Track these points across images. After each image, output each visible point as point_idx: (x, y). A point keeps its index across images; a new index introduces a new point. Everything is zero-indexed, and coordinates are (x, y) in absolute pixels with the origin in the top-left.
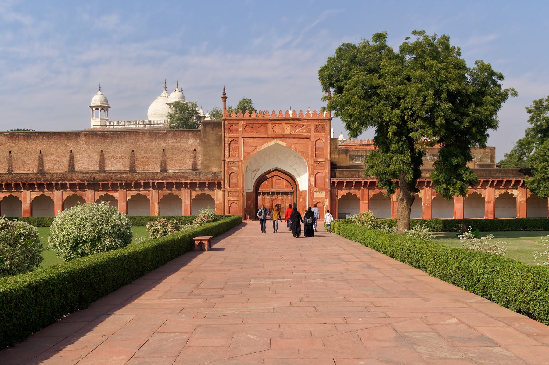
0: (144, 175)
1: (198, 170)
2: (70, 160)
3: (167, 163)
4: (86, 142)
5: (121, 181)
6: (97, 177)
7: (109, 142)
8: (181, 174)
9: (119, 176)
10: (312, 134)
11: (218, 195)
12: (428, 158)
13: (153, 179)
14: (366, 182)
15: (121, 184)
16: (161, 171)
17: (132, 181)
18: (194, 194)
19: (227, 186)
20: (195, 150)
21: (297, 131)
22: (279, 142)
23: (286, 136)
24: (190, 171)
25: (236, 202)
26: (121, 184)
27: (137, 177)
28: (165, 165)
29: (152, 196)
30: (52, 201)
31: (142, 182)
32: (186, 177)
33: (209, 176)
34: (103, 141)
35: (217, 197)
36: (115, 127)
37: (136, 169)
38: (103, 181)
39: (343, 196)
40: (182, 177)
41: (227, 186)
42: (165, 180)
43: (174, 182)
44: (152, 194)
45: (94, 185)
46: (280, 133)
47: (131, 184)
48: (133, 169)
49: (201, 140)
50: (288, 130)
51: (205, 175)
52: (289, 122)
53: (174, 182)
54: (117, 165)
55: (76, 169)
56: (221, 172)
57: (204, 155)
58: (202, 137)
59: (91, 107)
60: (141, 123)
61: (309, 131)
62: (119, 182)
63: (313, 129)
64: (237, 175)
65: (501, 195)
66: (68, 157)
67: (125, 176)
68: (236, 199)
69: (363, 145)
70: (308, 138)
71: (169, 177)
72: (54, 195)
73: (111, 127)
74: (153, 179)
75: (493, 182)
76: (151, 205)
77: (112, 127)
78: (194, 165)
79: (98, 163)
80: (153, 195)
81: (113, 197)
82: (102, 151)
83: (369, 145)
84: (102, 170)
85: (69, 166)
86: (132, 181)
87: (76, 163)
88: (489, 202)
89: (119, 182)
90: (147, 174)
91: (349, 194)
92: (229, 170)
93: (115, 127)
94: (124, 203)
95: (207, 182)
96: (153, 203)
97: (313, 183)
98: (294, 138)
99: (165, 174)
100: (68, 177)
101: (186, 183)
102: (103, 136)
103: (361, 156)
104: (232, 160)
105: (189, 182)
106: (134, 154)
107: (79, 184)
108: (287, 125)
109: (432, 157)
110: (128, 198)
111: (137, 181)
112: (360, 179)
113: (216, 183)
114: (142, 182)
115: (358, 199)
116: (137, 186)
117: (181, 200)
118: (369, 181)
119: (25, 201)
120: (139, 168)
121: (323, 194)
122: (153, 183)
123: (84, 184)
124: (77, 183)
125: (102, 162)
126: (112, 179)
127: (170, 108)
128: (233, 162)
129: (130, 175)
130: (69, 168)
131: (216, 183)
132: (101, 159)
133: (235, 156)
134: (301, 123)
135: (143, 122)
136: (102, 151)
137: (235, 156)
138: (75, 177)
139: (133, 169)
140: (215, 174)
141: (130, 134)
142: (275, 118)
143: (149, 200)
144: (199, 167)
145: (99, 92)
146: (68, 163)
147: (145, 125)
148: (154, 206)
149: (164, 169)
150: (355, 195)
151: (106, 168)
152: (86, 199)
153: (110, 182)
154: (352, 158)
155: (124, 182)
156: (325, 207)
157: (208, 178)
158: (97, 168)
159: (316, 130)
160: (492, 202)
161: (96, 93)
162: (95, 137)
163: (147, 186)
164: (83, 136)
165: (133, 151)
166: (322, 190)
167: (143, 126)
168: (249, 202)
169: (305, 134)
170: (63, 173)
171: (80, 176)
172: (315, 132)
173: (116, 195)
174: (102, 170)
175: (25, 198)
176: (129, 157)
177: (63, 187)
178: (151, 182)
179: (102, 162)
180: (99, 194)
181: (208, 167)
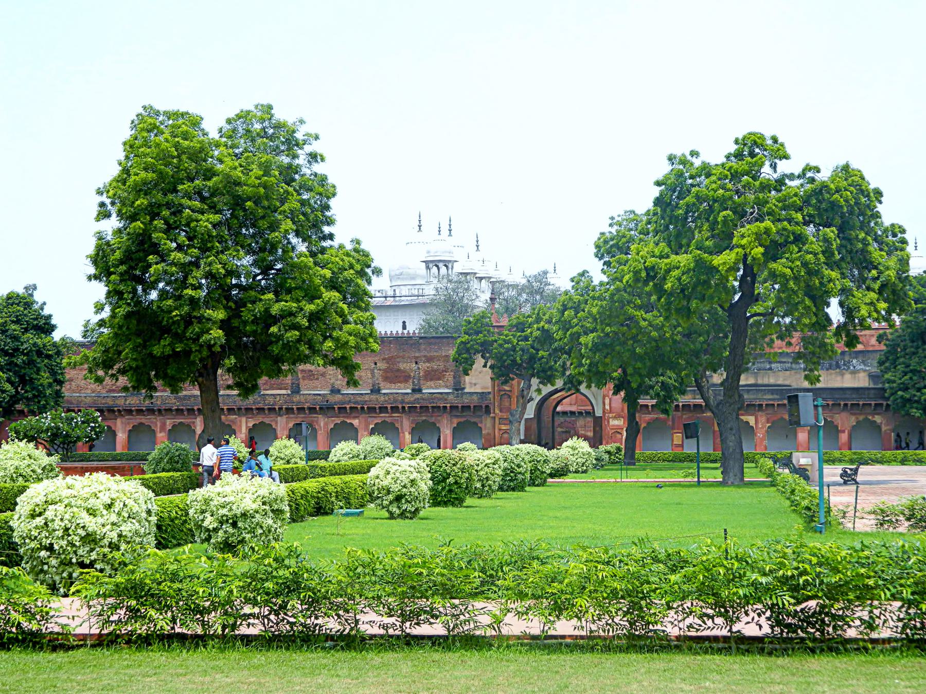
13: (403, 402)
15: (362, 408)
18: (456, 421)
19: (497, 411)
26: (362, 408)
29: (402, 425)
30: (275, 430)
31: (389, 406)
33: (475, 397)
40: (440, 399)
41: (497, 411)
45: (326, 409)
48: (376, 390)
56: (489, 393)
64: (510, 397)
67: (367, 398)
72: (277, 423)
74: (403, 402)
75: (846, 405)
81: (352, 424)
88: (843, 431)
92: (500, 391)
95: (472, 406)
97: (607, 407)
99: (418, 396)
101: (445, 407)
107: (310, 409)
110: (371, 426)
114: (389, 406)
116: (383, 409)
117: (439, 429)
119: (241, 431)
121: (619, 422)
122: (403, 408)
127: (428, 268)
129: (374, 397)
148: (404, 437)
163: (395, 409)
166: (617, 417)
173: (356, 422)
175: (241, 426)
177: (289, 410)
178: (400, 406)
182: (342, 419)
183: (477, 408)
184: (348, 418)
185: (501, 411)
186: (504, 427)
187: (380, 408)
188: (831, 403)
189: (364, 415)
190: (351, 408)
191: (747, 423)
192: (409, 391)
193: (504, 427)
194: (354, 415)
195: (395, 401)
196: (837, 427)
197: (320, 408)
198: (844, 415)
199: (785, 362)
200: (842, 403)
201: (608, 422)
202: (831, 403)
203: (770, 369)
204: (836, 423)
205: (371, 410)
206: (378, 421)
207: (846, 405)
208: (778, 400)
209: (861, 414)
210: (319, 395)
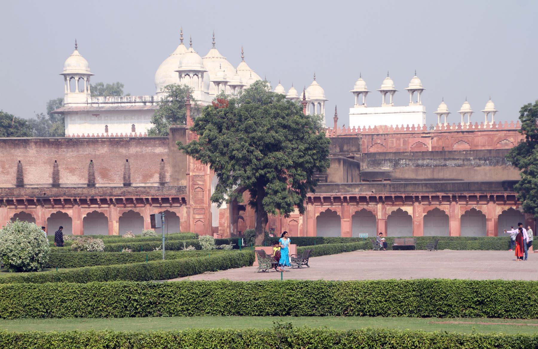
0: (100, 190)
1: (167, 183)
2: (18, 171)
3: (131, 175)
4: (37, 151)
5: (75, 197)
6: (48, 193)
7: (64, 152)
8: (142, 189)
9: (73, 192)
11: (182, 212)
12: (473, 162)
13: (111, 195)
14: (345, 198)
16: (125, 185)
17: (87, 197)
20: (162, 160)
24: (156, 185)
25: (202, 220)
27: (93, 192)
28: (129, 177)
29: (110, 214)
31: (98, 198)
32: (148, 193)
33: (174, 192)
34: (56, 150)
35: (182, 215)
36: (100, 105)
37: (96, 182)
38: (55, 197)
39: (322, 213)
40: (143, 193)
41: (192, 203)
42: (124, 196)
43: (134, 198)
44: (110, 212)
45: (44, 201)
47: (86, 200)
48: (91, 184)
49: (169, 148)
51: (169, 190)
54: (72, 180)
55: (26, 181)
57: (174, 166)
58: (170, 145)
59: (65, 75)
60: (138, 100)
62: (72, 199)
65: (504, 212)
66: (15, 169)
67: (79, 191)
68: (201, 216)
69: (463, 132)
71: (129, 192)
73: (94, 105)
75: (492, 197)
76: (110, 223)
77: (96, 105)
78: (162, 177)
79: (51, 175)
80: (114, 213)
81: (66, 214)
82: (56, 161)
83: (472, 132)
84: (56, 184)
85: (18, 178)
86: (87, 197)
87: (25, 175)
89: (72, 199)
90: (105, 189)
91: (328, 210)
93: (100, 105)
94: (79, 222)
95: (170, 198)
96: (112, 222)
99: (130, 189)
100: (15, 193)
101: (147, 199)
102: (56, 144)
103: (389, 160)
104: (197, 174)
105: (150, 198)
106: (93, 165)
109: (478, 161)
111: (93, 197)
112: (339, 194)
113: (180, 199)
115: (339, 216)
116: (93, 201)
117: (142, 217)
118: (348, 196)
120: (100, 182)
122: (111, 200)
123: (33, 200)
124: (24, 199)
125: (56, 175)
126: (65, 194)
127: (180, 76)
128: (198, 176)
130: (18, 182)
131: (180, 199)
132: (54, 171)
133: (200, 170)
135: (140, 98)
136: (56, 161)
137: (200, 170)
138: (22, 193)
139: (91, 184)
140: (181, 189)
141: (87, 142)
143: (106, 218)
144: (168, 179)
145: (76, 52)
146: (15, 175)
147: (145, 103)
148: (112, 224)
149: (127, 184)
150: (335, 212)
151: (61, 181)
152: (35, 217)
153: (62, 198)
154: (377, 163)
155: (78, 199)
156: (299, 225)
157: (171, 194)
158: (51, 181)
160: (493, 220)
161: (70, 55)
162: (47, 146)
163: (104, 201)
164: (33, 143)
165: (92, 161)
167: (142, 104)
168: (223, 221)
170: (9, 188)
171: (28, 191)
173: (70, 212)
174: (56, 184)
176: (87, 168)
178: (108, 198)
179: (56, 175)
180: (50, 211)
181: (178, 180)
182: (58, 210)
183: (175, 200)
184: (63, 208)
185: (195, 202)
186: (197, 217)
187: (173, 199)
188: (478, 195)
189: (76, 206)
190: (65, 200)
191: (406, 212)
192: (122, 185)
193: (197, 217)
194: (67, 206)
195: (105, 194)
196: (485, 216)
197: (38, 201)
198: (491, 204)
199: (458, 159)
200: (489, 195)
202: (478, 195)
203: (445, 165)
204: (483, 213)
205: (83, 202)
206: (90, 210)
207: (492, 197)
208: (432, 192)
209: (505, 204)
210: (37, 188)
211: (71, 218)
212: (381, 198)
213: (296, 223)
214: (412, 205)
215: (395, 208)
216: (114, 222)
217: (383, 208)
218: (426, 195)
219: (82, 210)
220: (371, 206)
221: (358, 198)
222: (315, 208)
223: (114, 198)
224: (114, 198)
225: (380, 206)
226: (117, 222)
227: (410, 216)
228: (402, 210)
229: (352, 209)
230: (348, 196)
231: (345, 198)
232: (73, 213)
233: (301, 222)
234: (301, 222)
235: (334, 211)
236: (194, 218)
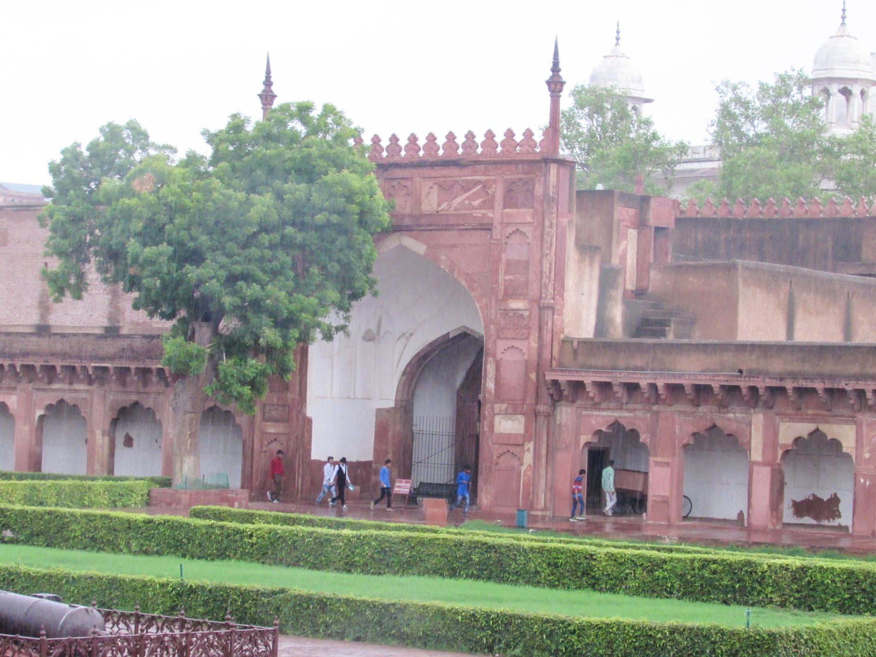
10: (496, 215)
21: (458, 200)
22: (408, 242)
23: (424, 221)
46: (408, 211)
50: (431, 201)
52: (432, 173)
53: (133, 366)
61: (489, 204)
63: (498, 191)
67: (19, 345)
70: (487, 227)
94: (26, 429)
98: (448, 227)
108: (430, 184)
115: (643, 445)
134: (467, 176)
142: (415, 160)
156: (523, 468)
159: (510, 200)
169: (478, 213)
172: (505, 207)
193: (272, 429)
201: (492, 426)
211: (11, 416)
212: (753, 390)
213: (517, 463)
214: (852, 420)
215: (803, 429)
216: (98, 432)
217: (766, 428)
218: (809, 385)
219: (37, 396)
220: (732, 418)
221: (716, 390)
222: (579, 417)
223: (18, 364)
224: (18, 364)
225: (758, 419)
226: (103, 435)
227: (848, 456)
228: (823, 436)
229: (681, 422)
230: (660, 383)
231: (653, 387)
232: (19, 401)
233: (528, 458)
234: (528, 458)
235: (633, 430)
236: (263, 433)
